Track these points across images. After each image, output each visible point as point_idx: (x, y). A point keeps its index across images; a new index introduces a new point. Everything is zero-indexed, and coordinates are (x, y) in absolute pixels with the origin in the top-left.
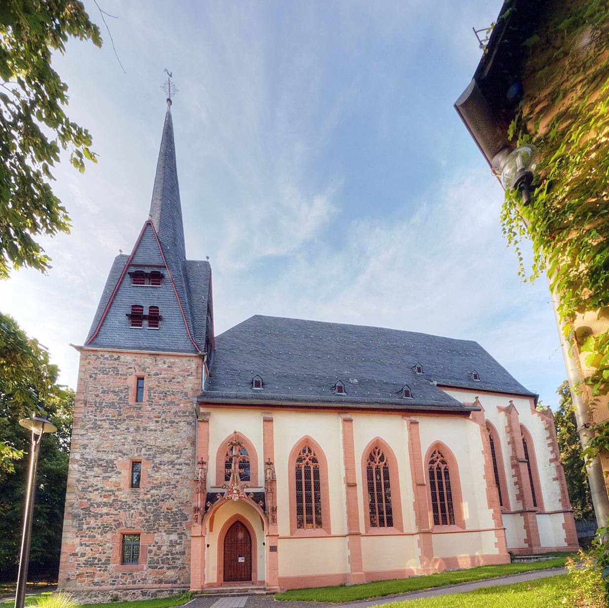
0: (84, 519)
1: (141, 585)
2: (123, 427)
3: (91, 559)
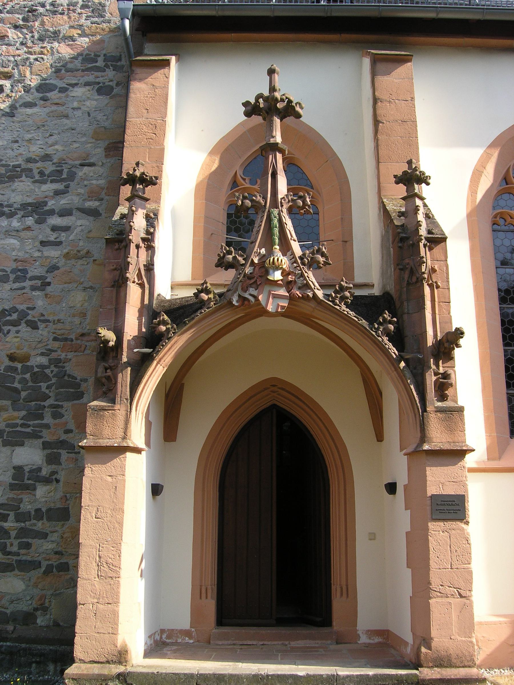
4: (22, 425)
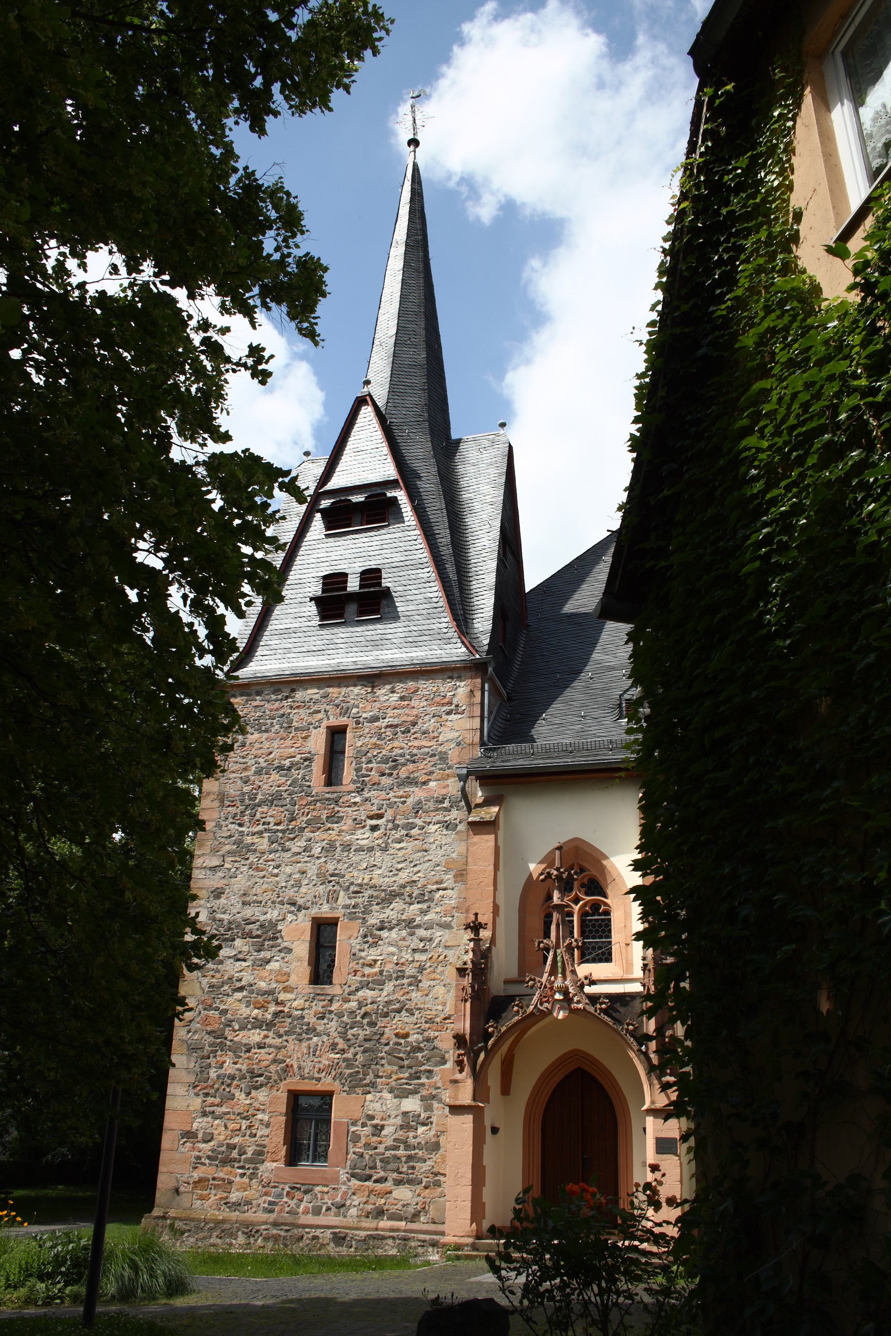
0: (211, 1055)
1: (331, 1219)
2: (297, 845)
3: (224, 1149)
4: (406, 1084)
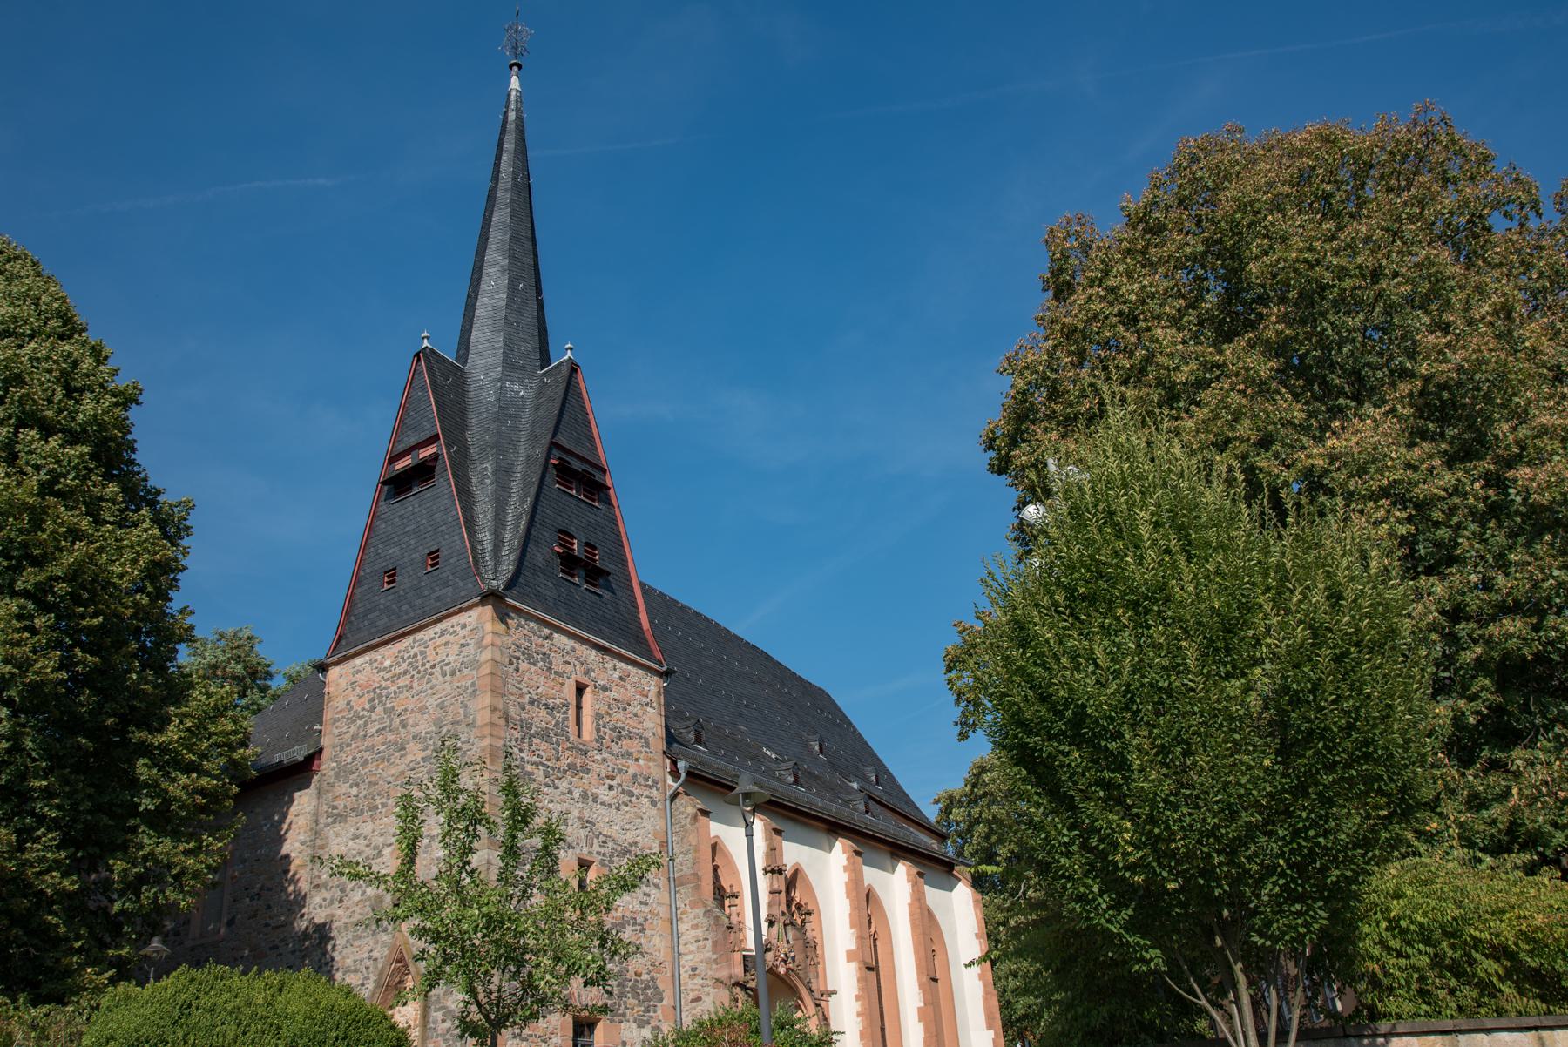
2: (563, 785)
